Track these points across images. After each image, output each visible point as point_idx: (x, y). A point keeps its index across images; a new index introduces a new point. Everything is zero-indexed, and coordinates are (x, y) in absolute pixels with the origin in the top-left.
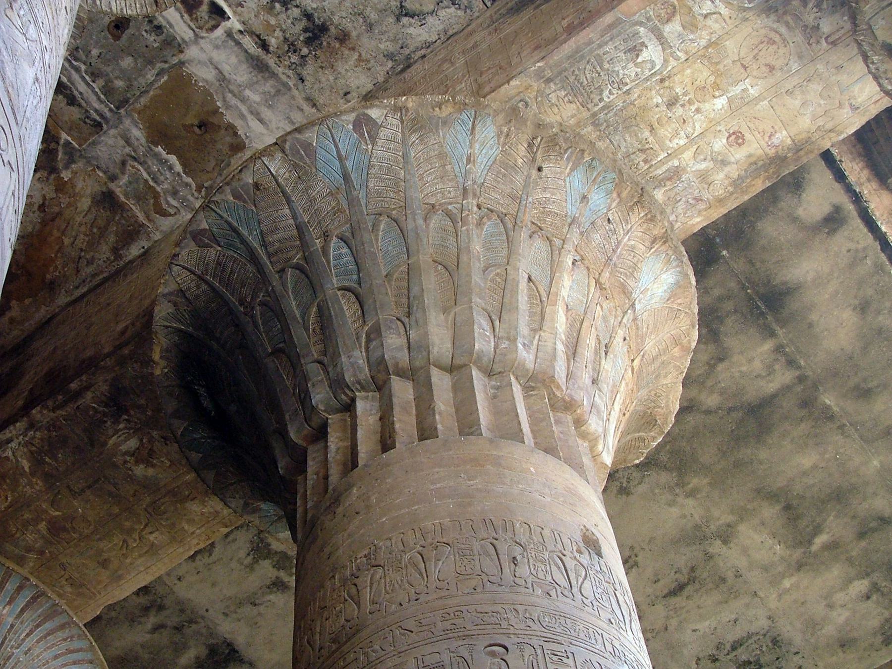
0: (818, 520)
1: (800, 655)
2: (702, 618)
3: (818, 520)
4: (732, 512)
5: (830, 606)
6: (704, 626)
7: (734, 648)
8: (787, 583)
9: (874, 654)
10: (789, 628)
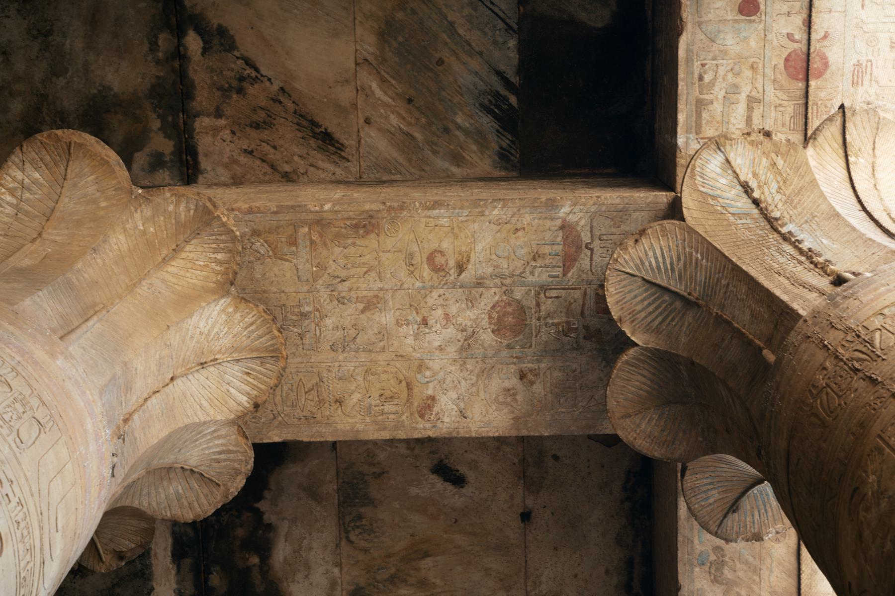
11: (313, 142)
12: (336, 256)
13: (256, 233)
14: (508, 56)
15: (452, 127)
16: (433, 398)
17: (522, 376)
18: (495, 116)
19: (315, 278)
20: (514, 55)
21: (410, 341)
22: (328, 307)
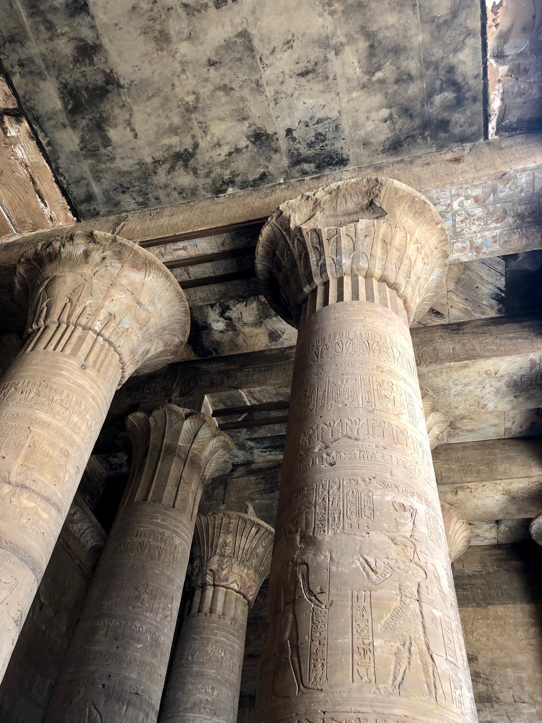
0: (382, 62)
1: (345, 141)
2: (310, 96)
3: (382, 62)
4: (346, 36)
5: (368, 118)
6: (310, 102)
7: (318, 123)
8: (354, 95)
9: (376, 156)
10: (346, 122)
11: (433, 315)
12: (455, 375)
13: (429, 372)
14: (502, 283)
17: (515, 397)
20: (504, 282)
21: (479, 392)
22: (452, 386)
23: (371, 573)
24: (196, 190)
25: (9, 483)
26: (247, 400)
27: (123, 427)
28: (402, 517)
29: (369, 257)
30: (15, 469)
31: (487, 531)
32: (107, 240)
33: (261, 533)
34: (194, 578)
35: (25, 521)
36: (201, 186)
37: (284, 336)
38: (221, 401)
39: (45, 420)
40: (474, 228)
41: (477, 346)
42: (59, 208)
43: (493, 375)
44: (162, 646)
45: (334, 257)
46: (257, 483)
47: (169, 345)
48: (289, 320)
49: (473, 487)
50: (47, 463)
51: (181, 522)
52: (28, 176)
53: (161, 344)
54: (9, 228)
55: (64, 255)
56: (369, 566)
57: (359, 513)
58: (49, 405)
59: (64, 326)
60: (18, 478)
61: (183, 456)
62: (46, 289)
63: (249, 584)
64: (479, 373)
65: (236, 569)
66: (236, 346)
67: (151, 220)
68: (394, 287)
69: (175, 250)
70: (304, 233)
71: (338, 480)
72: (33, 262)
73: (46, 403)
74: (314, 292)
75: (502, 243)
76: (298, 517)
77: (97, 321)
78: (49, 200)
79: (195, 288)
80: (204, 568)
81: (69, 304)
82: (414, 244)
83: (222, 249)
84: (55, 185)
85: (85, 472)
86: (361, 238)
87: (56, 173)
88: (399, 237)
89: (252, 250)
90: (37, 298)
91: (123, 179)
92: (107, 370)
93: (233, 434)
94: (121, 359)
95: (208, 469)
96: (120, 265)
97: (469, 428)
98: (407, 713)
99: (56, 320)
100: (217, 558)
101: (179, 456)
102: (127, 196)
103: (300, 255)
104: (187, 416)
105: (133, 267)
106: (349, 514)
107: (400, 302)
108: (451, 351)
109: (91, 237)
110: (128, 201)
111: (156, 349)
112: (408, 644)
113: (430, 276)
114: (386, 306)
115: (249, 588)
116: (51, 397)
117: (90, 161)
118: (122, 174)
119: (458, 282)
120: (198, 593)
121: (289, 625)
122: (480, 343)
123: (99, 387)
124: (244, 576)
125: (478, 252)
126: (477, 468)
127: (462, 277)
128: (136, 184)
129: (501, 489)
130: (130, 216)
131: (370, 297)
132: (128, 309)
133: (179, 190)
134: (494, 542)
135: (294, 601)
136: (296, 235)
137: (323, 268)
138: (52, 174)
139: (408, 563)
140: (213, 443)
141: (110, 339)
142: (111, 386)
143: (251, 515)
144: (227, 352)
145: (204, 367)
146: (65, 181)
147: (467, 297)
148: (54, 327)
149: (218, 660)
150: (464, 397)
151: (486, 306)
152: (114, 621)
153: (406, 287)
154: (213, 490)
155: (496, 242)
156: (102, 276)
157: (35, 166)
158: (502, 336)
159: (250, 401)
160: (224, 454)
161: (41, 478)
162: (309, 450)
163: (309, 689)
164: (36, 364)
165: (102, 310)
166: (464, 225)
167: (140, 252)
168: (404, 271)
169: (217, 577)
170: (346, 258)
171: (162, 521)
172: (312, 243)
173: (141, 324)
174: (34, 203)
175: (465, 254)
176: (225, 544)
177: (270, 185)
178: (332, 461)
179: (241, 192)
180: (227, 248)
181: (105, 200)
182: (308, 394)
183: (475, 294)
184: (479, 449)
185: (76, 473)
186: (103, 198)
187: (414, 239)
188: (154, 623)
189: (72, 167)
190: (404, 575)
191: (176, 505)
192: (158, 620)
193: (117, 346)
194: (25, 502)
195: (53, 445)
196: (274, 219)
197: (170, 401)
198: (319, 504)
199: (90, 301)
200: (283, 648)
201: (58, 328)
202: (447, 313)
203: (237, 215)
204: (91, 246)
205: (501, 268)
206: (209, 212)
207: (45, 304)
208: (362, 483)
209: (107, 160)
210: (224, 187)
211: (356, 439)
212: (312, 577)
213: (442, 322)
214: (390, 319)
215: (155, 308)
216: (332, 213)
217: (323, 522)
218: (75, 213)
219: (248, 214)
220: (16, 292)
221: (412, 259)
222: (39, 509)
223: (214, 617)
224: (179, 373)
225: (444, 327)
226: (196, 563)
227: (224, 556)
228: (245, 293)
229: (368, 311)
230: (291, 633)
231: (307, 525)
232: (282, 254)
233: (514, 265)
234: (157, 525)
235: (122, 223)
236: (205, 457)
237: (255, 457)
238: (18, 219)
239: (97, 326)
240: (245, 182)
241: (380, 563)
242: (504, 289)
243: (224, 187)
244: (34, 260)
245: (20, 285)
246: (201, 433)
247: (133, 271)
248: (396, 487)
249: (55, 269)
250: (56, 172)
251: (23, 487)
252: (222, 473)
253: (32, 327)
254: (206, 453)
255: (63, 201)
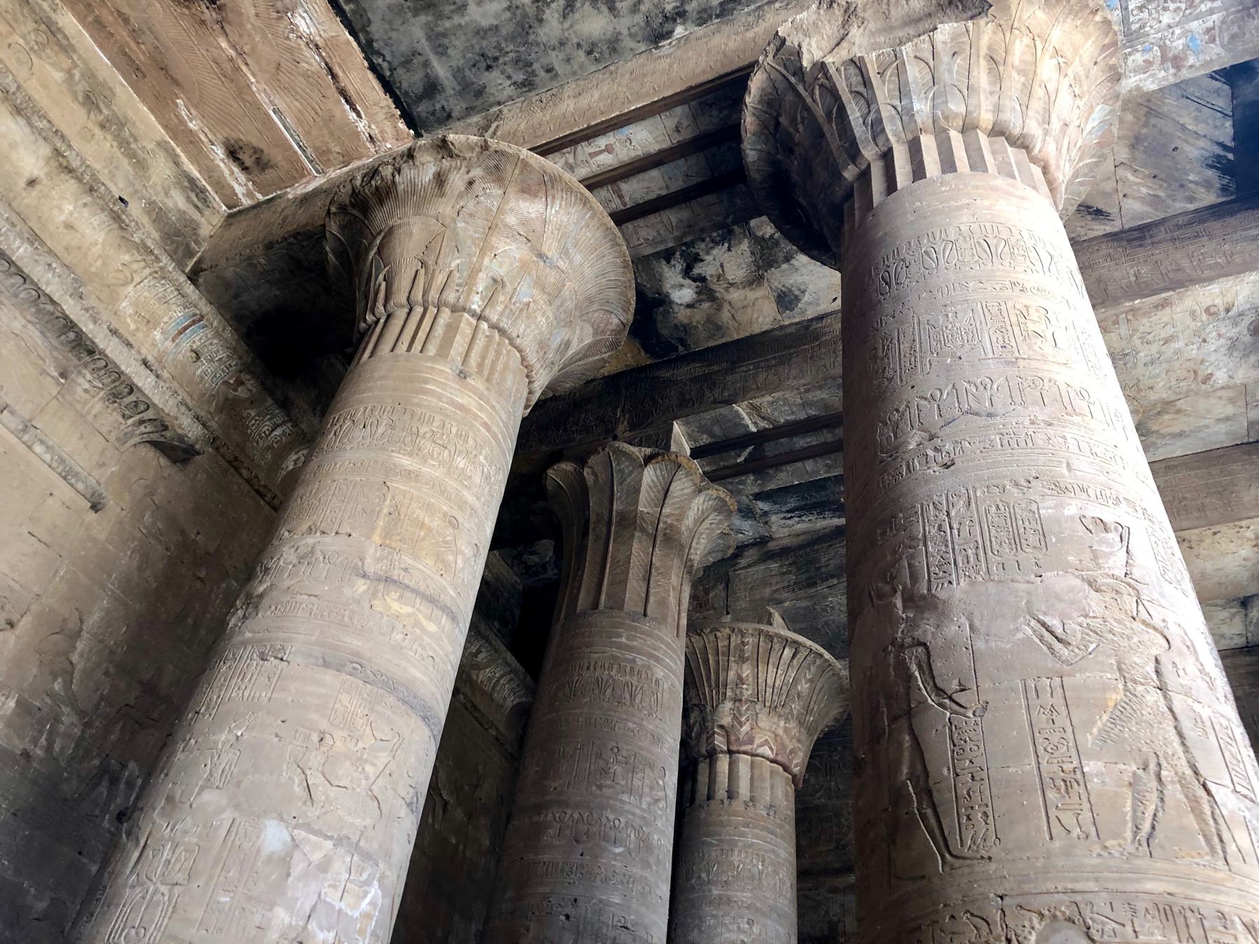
11: (1089, 217)
12: (1144, 324)
14: (1226, 131)
15: (1186, 183)
16: (1211, 374)
18: (1217, 168)
19: (1131, 336)
20: (1230, 131)
22: (1140, 347)
23: (1057, 646)
24: (617, 40)
25: (364, 576)
26: (749, 422)
27: (541, 492)
28: (1101, 542)
29: (965, 92)
30: (371, 552)
31: (1223, 621)
32: (471, 148)
33: (800, 656)
34: (693, 743)
35: (400, 637)
36: (625, 32)
37: (807, 298)
38: (703, 430)
39: (411, 468)
40: (1166, 18)
41: (1185, 263)
42: (381, 116)
43: (1223, 314)
44: (656, 851)
45: (897, 103)
46: (784, 574)
47: (603, 332)
48: (815, 253)
49: (1194, 537)
50: (423, 539)
51: (662, 641)
52: (323, 65)
53: (589, 330)
54: (303, 168)
55: (401, 188)
56: (1052, 633)
57: (1017, 542)
58: (413, 443)
59: (419, 310)
60: (378, 567)
61: (650, 530)
62: (379, 252)
63: (790, 747)
64: (1193, 314)
65: (764, 721)
66: (719, 328)
67: (542, 109)
68: (1021, 143)
69: (593, 155)
70: (832, 71)
71: (964, 491)
72: (350, 210)
73: (408, 440)
74: (865, 175)
75: (1226, 39)
76: (893, 566)
77: (473, 293)
78: (366, 108)
79: (636, 223)
80: (709, 724)
81: (422, 271)
82: (1052, 58)
83: (677, 138)
84: (370, 75)
85: (484, 582)
86: (946, 59)
87: (369, 52)
88: (1019, 48)
89: (733, 132)
90: (367, 270)
91: (484, 43)
92: (503, 379)
93: (730, 487)
94: (523, 359)
95: (696, 549)
96: (500, 192)
97: (1176, 429)
98: (1172, 889)
99: (404, 301)
100: (728, 705)
101: (643, 530)
102: (495, 73)
103: (829, 114)
104: (648, 460)
105: (523, 191)
106: (996, 547)
107: (1037, 171)
108: (1133, 279)
109: (443, 147)
110: (498, 83)
111: (581, 340)
112: (1152, 767)
113: (1087, 122)
114: (1013, 177)
115: (791, 752)
116: (414, 429)
117: (423, 18)
118: (481, 33)
119: (1135, 142)
120: (703, 767)
121: (906, 754)
122: (1190, 257)
123: (492, 407)
124: (781, 732)
125: (1178, 67)
126: (1199, 502)
127: (1143, 127)
128: (508, 49)
129: (1252, 536)
130: (505, 111)
131: (977, 164)
132: (524, 267)
133: (586, 47)
134: (1241, 642)
135: (907, 712)
136: (817, 79)
137: (877, 128)
138: (362, 55)
139: (1128, 624)
140: (699, 503)
141: (501, 325)
142: (513, 406)
143: (779, 626)
144: (704, 342)
145: (665, 374)
146: (385, 65)
147: (1156, 172)
148: (401, 314)
149: (753, 876)
150: (1165, 366)
151: (1197, 183)
152: (569, 812)
153: (1044, 141)
154: (707, 592)
155: (1213, 40)
156: (471, 215)
157: (332, 43)
158: (1235, 237)
159: (755, 423)
160: (720, 522)
161: (416, 565)
162: (895, 450)
163: (964, 858)
164: (381, 378)
165: (481, 275)
166: (1145, 15)
167: (532, 162)
168: (1037, 112)
169: (733, 738)
170: (920, 100)
171: (627, 639)
172: (849, 85)
173: (549, 294)
174: (338, 114)
175: (1153, 75)
176: (740, 680)
177: (753, 7)
178: (946, 460)
179: (700, 31)
180: (686, 135)
181: (458, 88)
182: (880, 353)
183: (1170, 164)
184: (1199, 468)
185: (475, 556)
186: (455, 83)
187: (1051, 49)
188: (638, 812)
189: (394, 35)
190: (1124, 643)
191: (648, 612)
192: (644, 806)
193: (514, 335)
194: (396, 607)
195: (429, 508)
196: (771, 56)
197: (615, 438)
198: (932, 538)
199: (458, 261)
200: (898, 796)
201: (409, 314)
202: (1116, 210)
203: (698, 71)
204: (446, 163)
205: (1223, 103)
206: (645, 75)
207: (381, 277)
208: (1015, 490)
209: (452, 12)
210: (667, 27)
211: (990, 415)
212: (938, 665)
213: (1109, 229)
214: (1023, 198)
215: (571, 262)
216: (880, 24)
217: (945, 568)
218: (411, 121)
219: (719, 65)
220: (331, 271)
221: (1051, 87)
222: (420, 616)
223: (738, 805)
224: (623, 391)
225: (1113, 237)
226: (694, 716)
227: (740, 700)
228: (726, 217)
229: (977, 187)
230: (912, 767)
231: (914, 578)
232: (793, 121)
233: (1248, 91)
234: (620, 646)
235: (494, 125)
236: (688, 528)
237: (774, 528)
238: (316, 149)
239: (476, 304)
240: (705, 10)
241: (1072, 626)
242: (1232, 144)
243: (667, 27)
244: (353, 205)
245: (335, 255)
246: (676, 487)
247: (524, 200)
248: (1082, 490)
249: (391, 215)
250: (368, 49)
251: (388, 580)
252: (719, 556)
253: (365, 321)
254: (689, 521)
255: (387, 101)
